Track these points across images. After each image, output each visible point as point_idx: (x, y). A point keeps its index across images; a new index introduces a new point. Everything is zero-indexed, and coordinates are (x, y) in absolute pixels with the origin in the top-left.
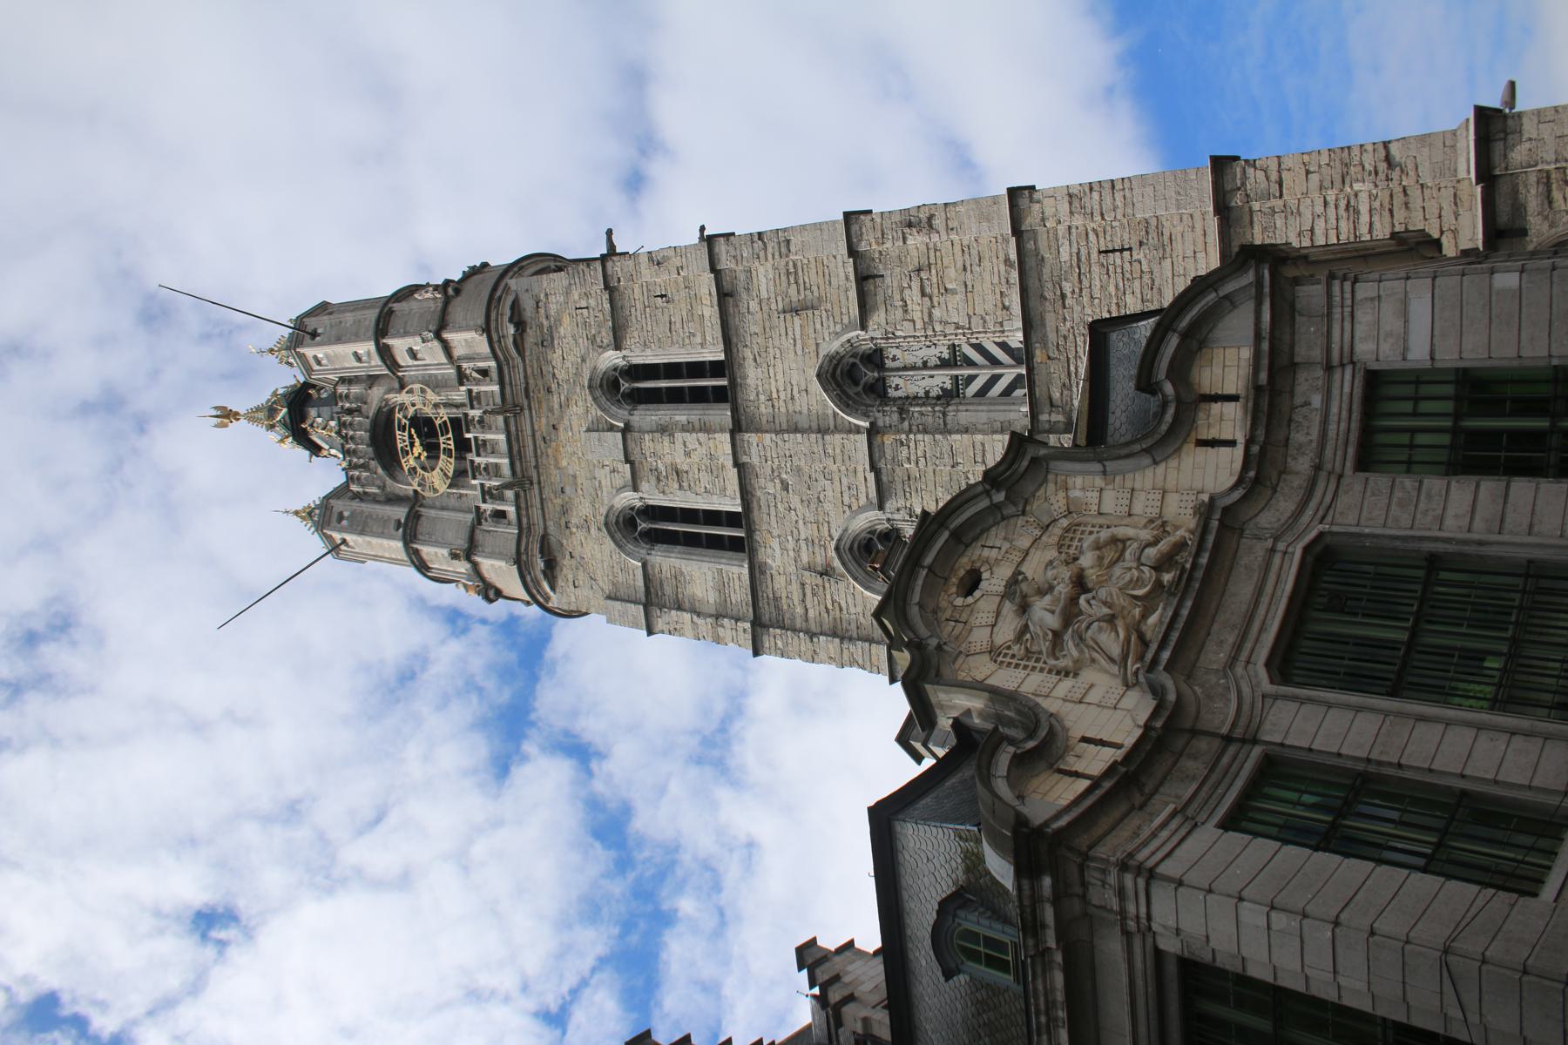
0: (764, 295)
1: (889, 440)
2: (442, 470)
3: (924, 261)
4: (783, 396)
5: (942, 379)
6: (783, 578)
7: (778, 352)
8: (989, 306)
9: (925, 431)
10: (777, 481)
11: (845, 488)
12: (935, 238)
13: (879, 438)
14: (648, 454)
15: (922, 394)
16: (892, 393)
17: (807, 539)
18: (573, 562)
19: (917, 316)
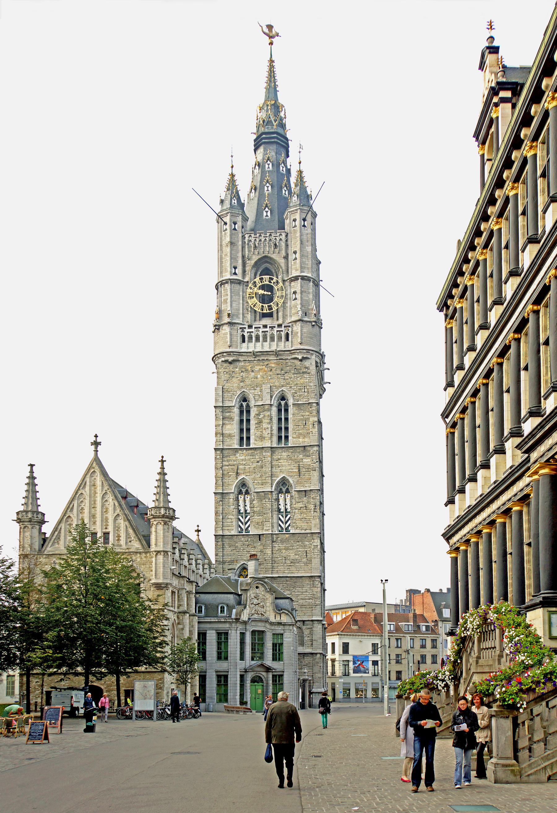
0: (304, 460)
1: (270, 496)
2: (256, 303)
3: (307, 509)
4: (280, 464)
5: (283, 510)
6: (235, 459)
7: (290, 463)
8: (298, 524)
9: (272, 506)
10: (259, 460)
11: (258, 481)
12: (312, 513)
13: (270, 494)
14: (264, 413)
15: (280, 503)
16: (280, 495)
17: (245, 468)
18: (231, 373)
19: (296, 506)
